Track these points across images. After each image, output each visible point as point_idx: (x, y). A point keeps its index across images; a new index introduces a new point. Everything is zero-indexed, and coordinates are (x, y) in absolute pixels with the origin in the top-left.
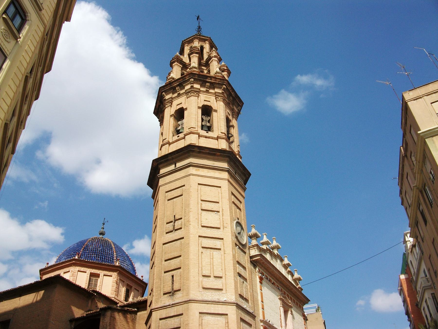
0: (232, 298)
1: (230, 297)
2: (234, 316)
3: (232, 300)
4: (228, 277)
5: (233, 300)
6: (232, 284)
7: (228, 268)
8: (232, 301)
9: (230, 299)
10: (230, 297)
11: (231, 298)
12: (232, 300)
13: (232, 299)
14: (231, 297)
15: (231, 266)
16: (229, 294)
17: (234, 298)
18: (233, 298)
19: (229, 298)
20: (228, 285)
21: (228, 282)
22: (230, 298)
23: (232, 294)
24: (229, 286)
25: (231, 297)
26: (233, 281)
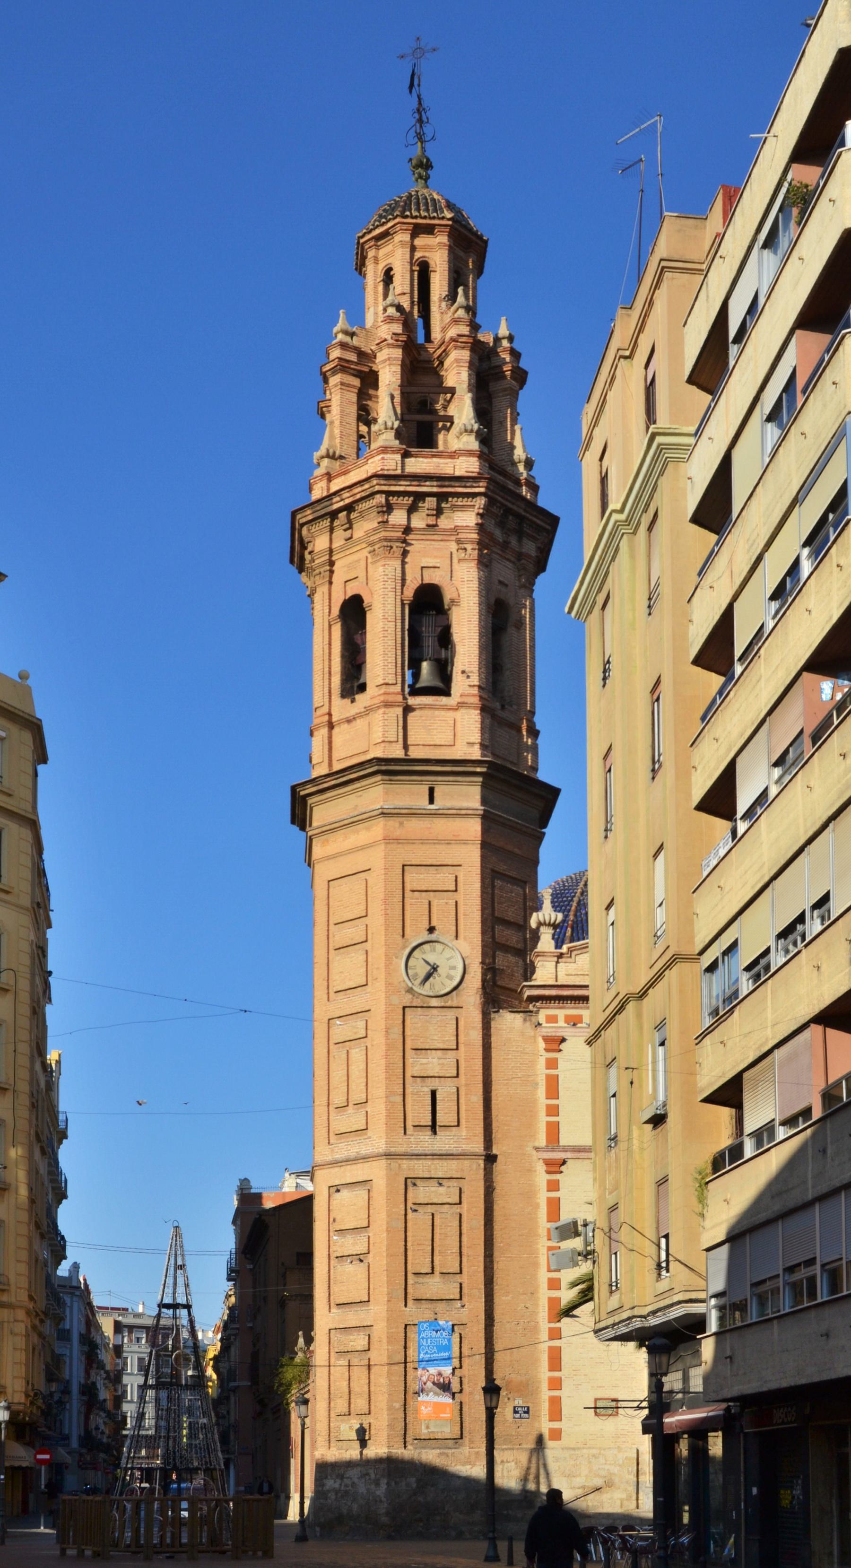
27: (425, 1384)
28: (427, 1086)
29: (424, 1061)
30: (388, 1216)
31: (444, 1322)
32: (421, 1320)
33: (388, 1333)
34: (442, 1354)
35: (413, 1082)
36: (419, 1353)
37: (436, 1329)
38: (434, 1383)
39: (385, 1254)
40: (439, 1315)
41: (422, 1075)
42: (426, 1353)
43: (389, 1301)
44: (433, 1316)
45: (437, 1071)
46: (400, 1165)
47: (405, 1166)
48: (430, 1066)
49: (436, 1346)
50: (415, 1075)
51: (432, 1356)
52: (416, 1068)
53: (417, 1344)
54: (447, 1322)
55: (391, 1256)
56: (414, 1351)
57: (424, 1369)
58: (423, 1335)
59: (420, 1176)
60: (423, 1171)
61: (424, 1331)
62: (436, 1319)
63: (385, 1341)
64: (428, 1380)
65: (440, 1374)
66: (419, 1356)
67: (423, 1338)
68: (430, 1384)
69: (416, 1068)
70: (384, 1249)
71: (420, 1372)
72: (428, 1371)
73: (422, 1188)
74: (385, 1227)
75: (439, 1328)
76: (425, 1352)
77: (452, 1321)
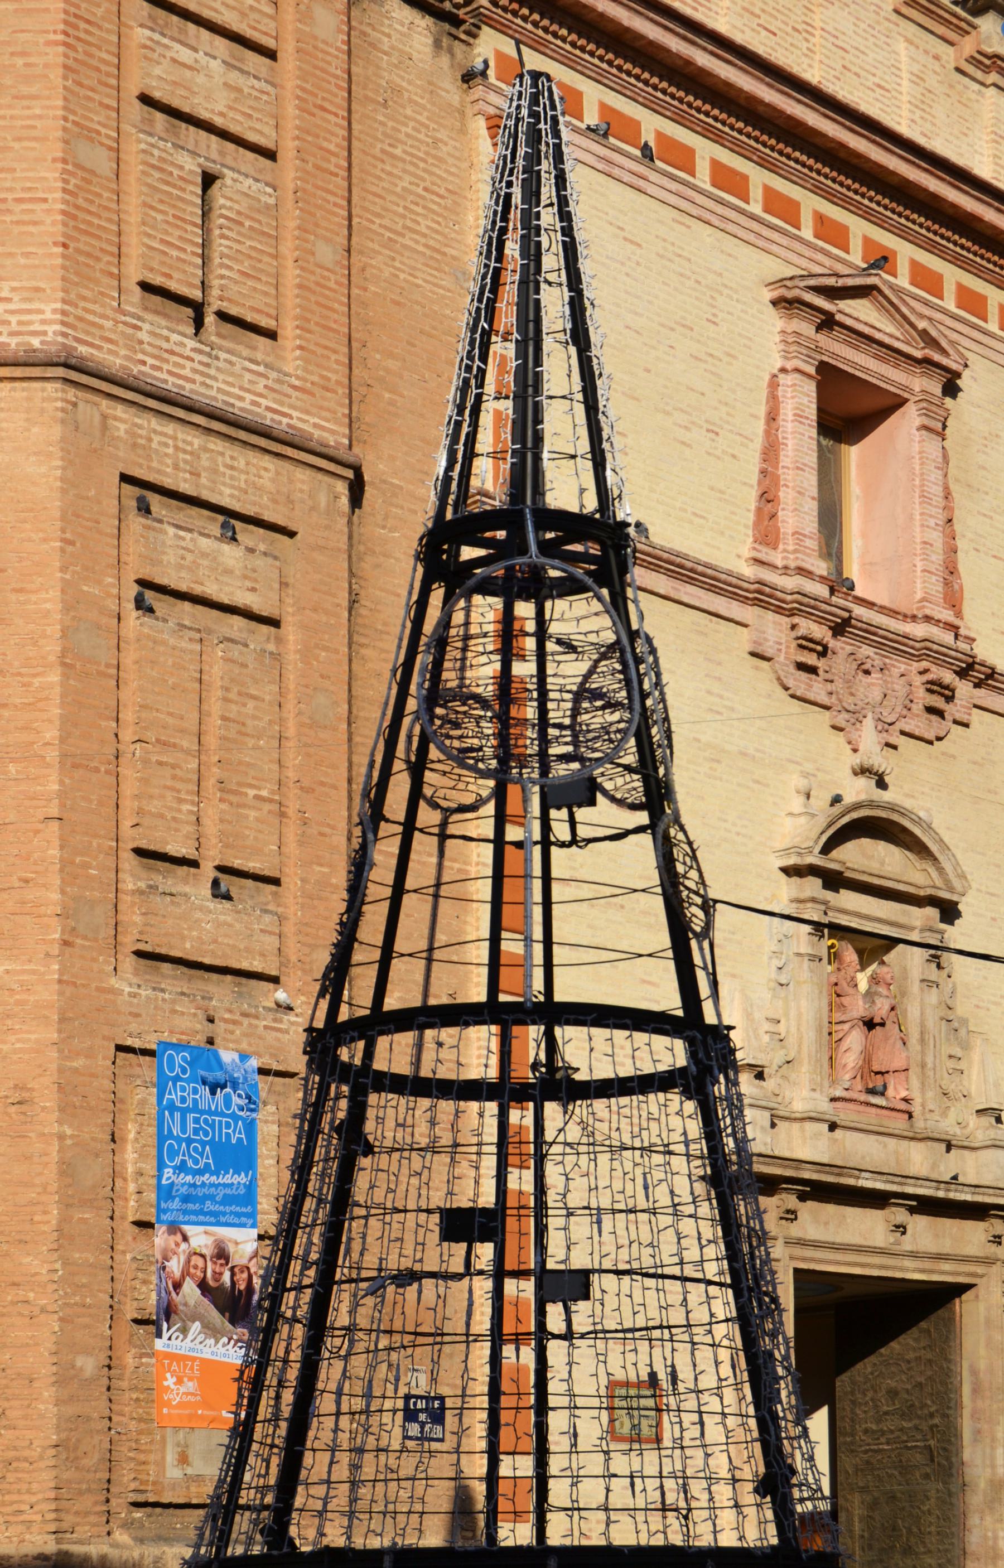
0: (29, 323)
1: (12, 312)
2: (43, 470)
3: (35, 333)
4: (16, 145)
5: (45, 333)
6: (45, 200)
7: (20, 62)
8: (36, 342)
9: (14, 327)
10: (12, 312)
11: (20, 323)
12: (35, 333)
13: (37, 327)
14: (29, 312)
15: (48, 43)
16: (14, 289)
17: (49, 315)
18: (43, 322)
19: (9, 323)
20: (9, 211)
21: (10, 190)
22: (14, 319)
23: (37, 290)
24: (18, 223)
25: (29, 312)
26: (51, 175)
27: (177, 1286)
28: (194, 154)
29: (185, 55)
30: (67, 608)
31: (236, 1056)
32: (166, 1037)
33: (61, 1070)
34: (228, 1179)
35: (143, 120)
36: (161, 1166)
37: (210, 1077)
38: (203, 1286)
39: (52, 755)
40: (220, 1027)
41: (176, 103)
42: (182, 1168)
43: (66, 943)
44: (200, 1029)
45: (220, 107)
46: (105, 417)
47: (121, 429)
48: (200, 79)
49: (212, 1143)
50: (157, 95)
51: (199, 1180)
52: (157, 71)
53: (153, 1130)
54: (244, 1057)
55: (75, 766)
56: (142, 1156)
57: (174, 1228)
58: (173, 1096)
59: (168, 482)
60: (176, 467)
61: (177, 1079)
62: (211, 1041)
63: (47, 1100)
64: (185, 1273)
65: (222, 1254)
66: (159, 1177)
67: (172, 1107)
68: (190, 1290)
69: (157, 71)
70: (51, 734)
71: (161, 1238)
72: (185, 1238)
73: (171, 531)
74: (52, 648)
75: (219, 1076)
76: (177, 1161)
77: (259, 1055)
